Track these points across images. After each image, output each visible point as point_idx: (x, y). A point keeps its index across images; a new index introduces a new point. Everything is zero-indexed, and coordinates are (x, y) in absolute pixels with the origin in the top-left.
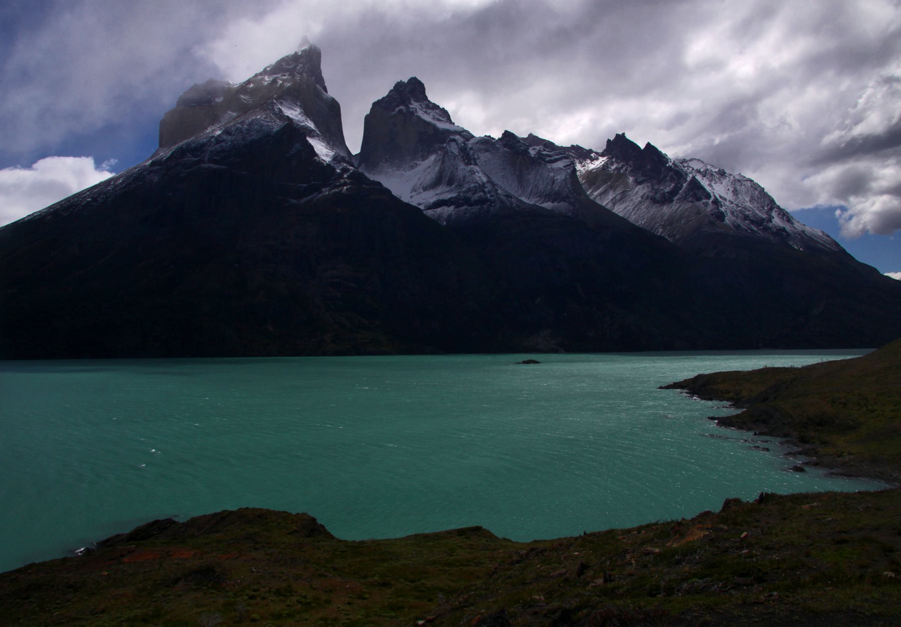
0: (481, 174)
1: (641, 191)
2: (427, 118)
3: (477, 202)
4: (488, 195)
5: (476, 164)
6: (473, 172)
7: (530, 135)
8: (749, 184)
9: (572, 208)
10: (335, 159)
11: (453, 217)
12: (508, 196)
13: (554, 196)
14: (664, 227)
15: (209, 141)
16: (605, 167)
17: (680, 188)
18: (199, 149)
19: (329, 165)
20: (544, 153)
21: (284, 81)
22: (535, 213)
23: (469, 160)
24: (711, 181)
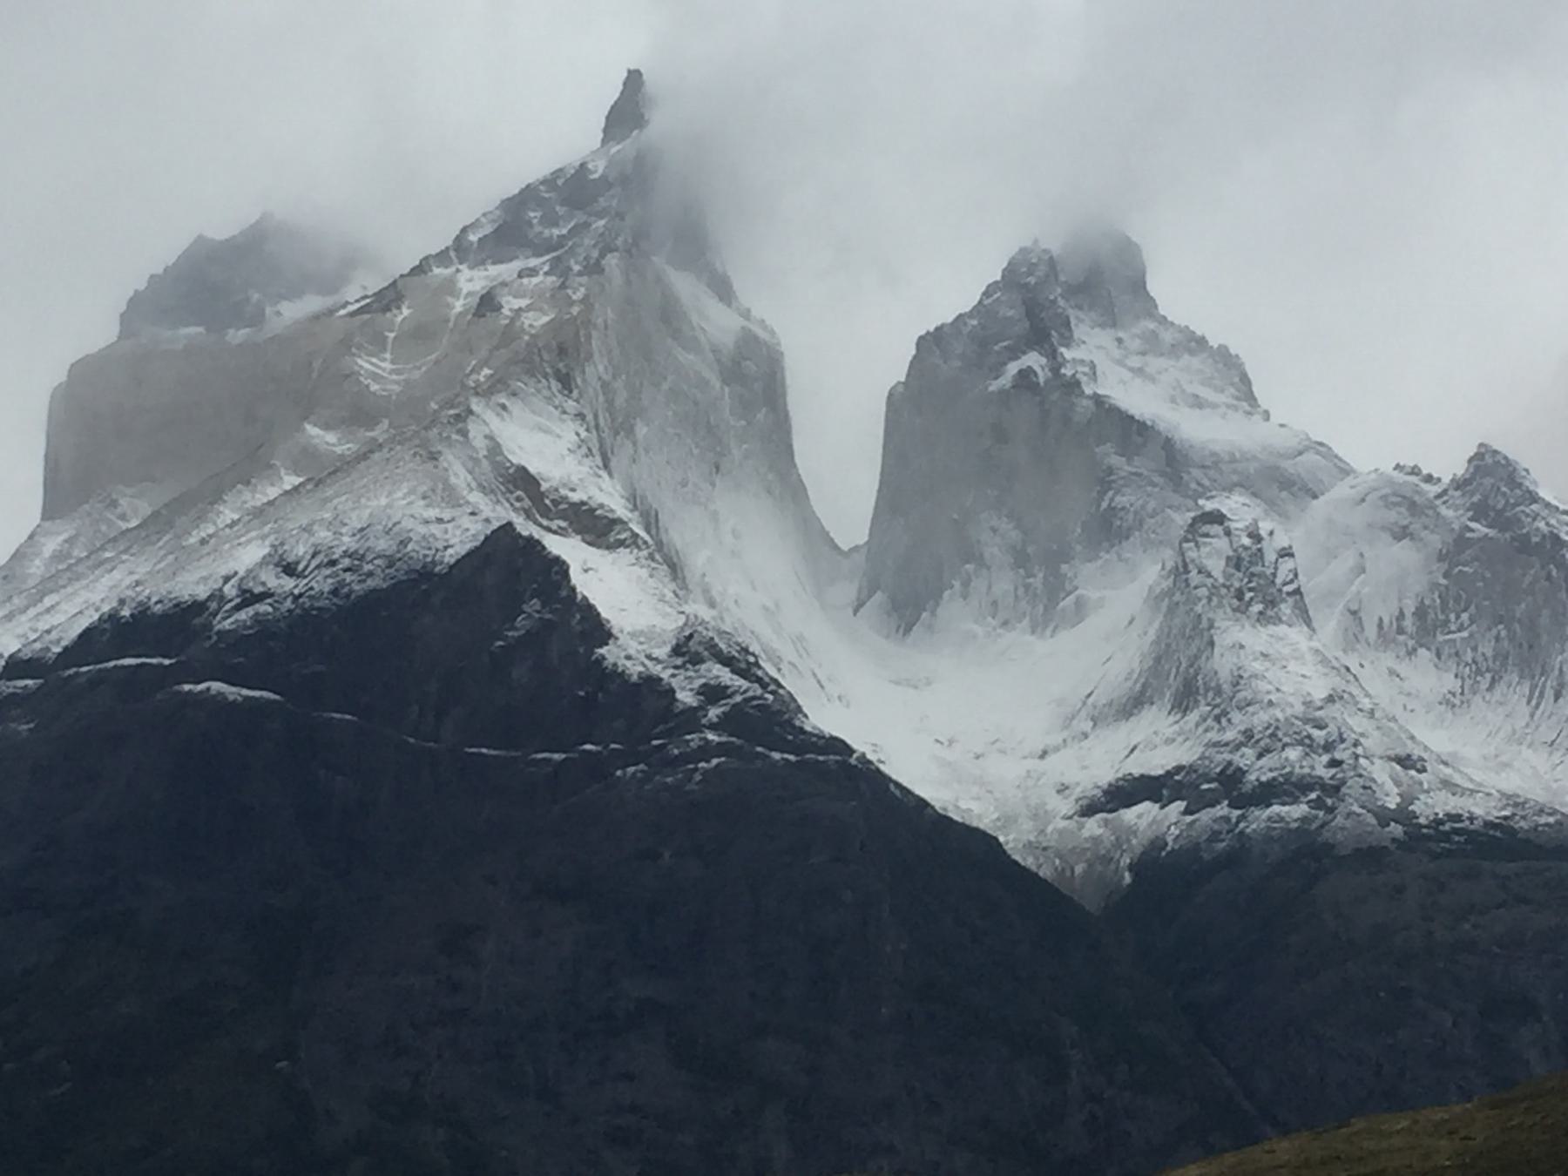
3: (1268, 793)
15: (217, 596)
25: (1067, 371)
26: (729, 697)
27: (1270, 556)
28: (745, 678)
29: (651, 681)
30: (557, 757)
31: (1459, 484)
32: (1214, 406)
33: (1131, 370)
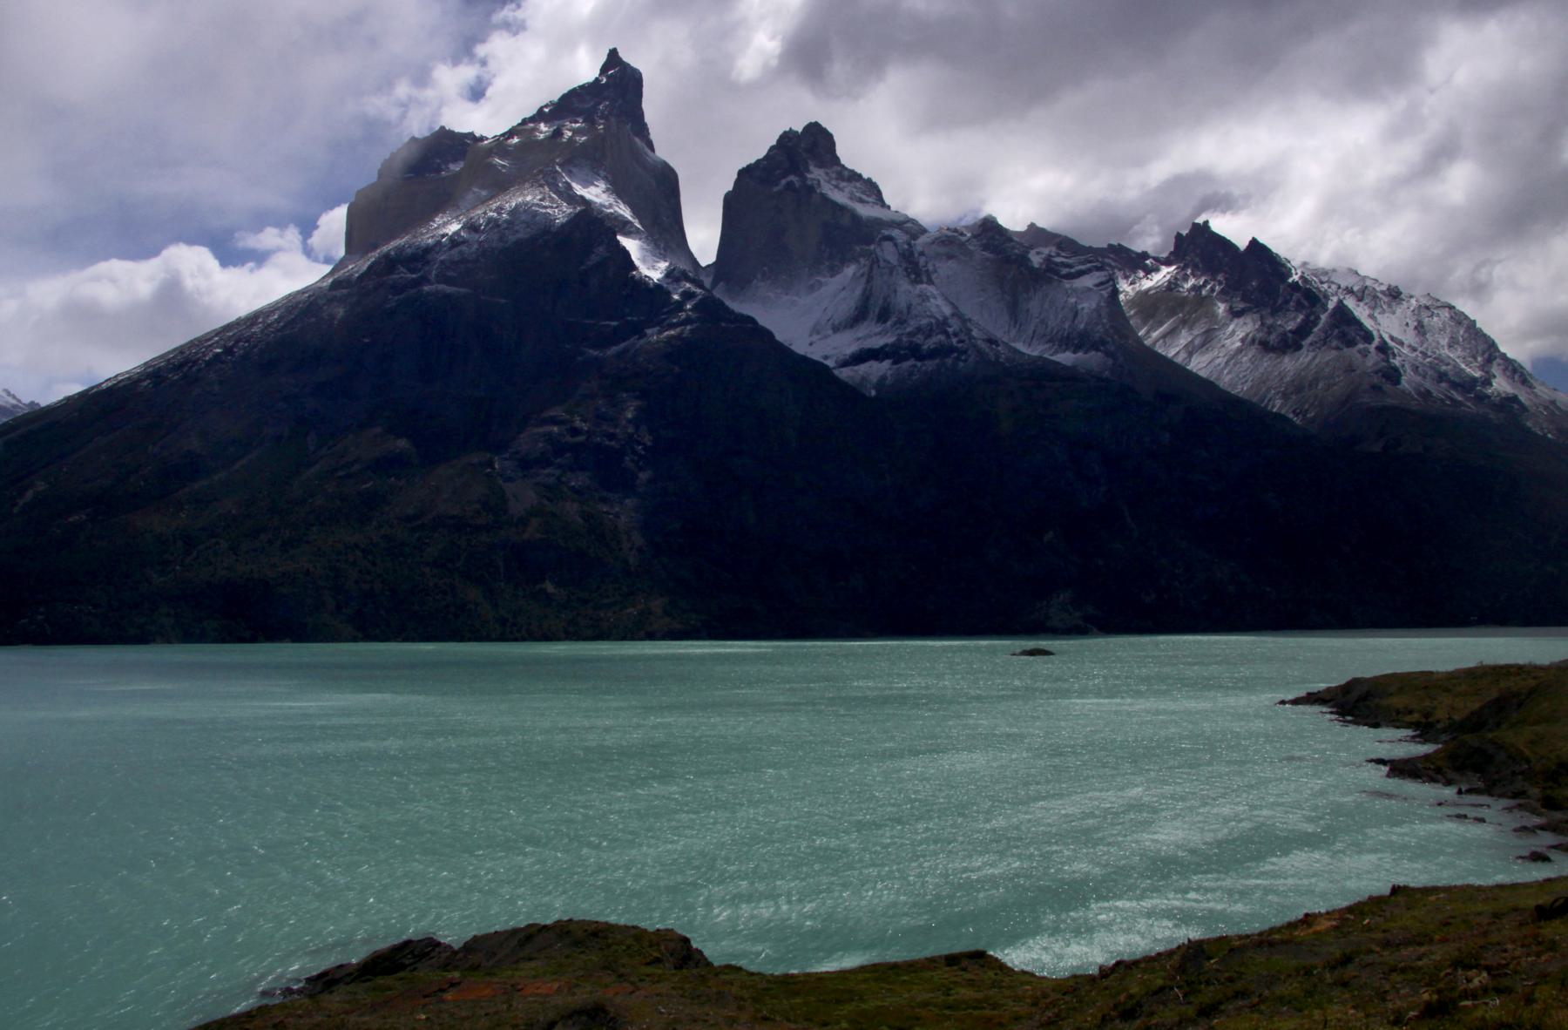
0: (940, 301)
1: (1237, 332)
2: (839, 197)
3: (932, 354)
4: (954, 340)
5: (930, 282)
6: (924, 298)
7: (1032, 226)
8: (1445, 314)
9: (1110, 362)
10: (669, 274)
11: (888, 382)
12: (992, 341)
13: (1079, 341)
14: (1285, 396)
15: (439, 243)
16: (1172, 286)
17: (1315, 323)
18: (421, 257)
19: (658, 287)
20: (1058, 260)
21: (576, 132)
22: (1043, 373)
23: (918, 275)
24: (1373, 308)
30: (615, 323)
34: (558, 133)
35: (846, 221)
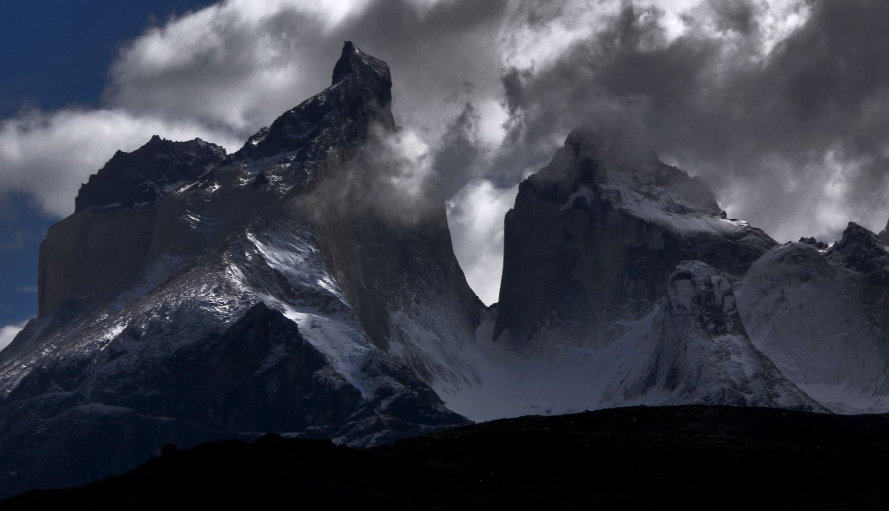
5: (740, 330)
15: (93, 355)
23: (719, 322)
25: (604, 197)
26: (393, 394)
27: (718, 296)
28: (403, 384)
29: (348, 388)
31: (837, 247)
32: (692, 211)
33: (642, 194)
34: (261, 180)
35: (656, 243)
